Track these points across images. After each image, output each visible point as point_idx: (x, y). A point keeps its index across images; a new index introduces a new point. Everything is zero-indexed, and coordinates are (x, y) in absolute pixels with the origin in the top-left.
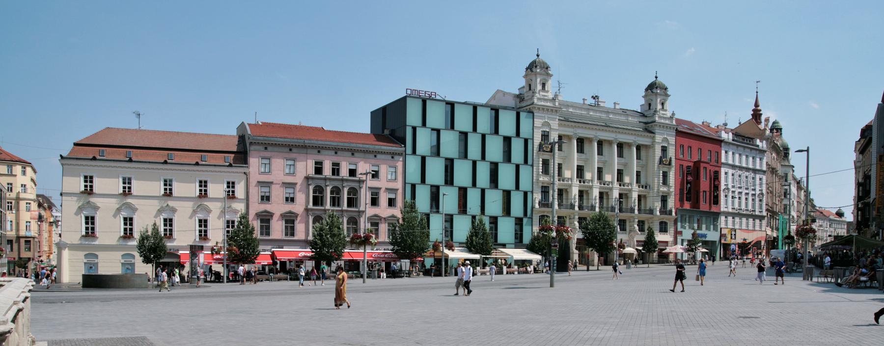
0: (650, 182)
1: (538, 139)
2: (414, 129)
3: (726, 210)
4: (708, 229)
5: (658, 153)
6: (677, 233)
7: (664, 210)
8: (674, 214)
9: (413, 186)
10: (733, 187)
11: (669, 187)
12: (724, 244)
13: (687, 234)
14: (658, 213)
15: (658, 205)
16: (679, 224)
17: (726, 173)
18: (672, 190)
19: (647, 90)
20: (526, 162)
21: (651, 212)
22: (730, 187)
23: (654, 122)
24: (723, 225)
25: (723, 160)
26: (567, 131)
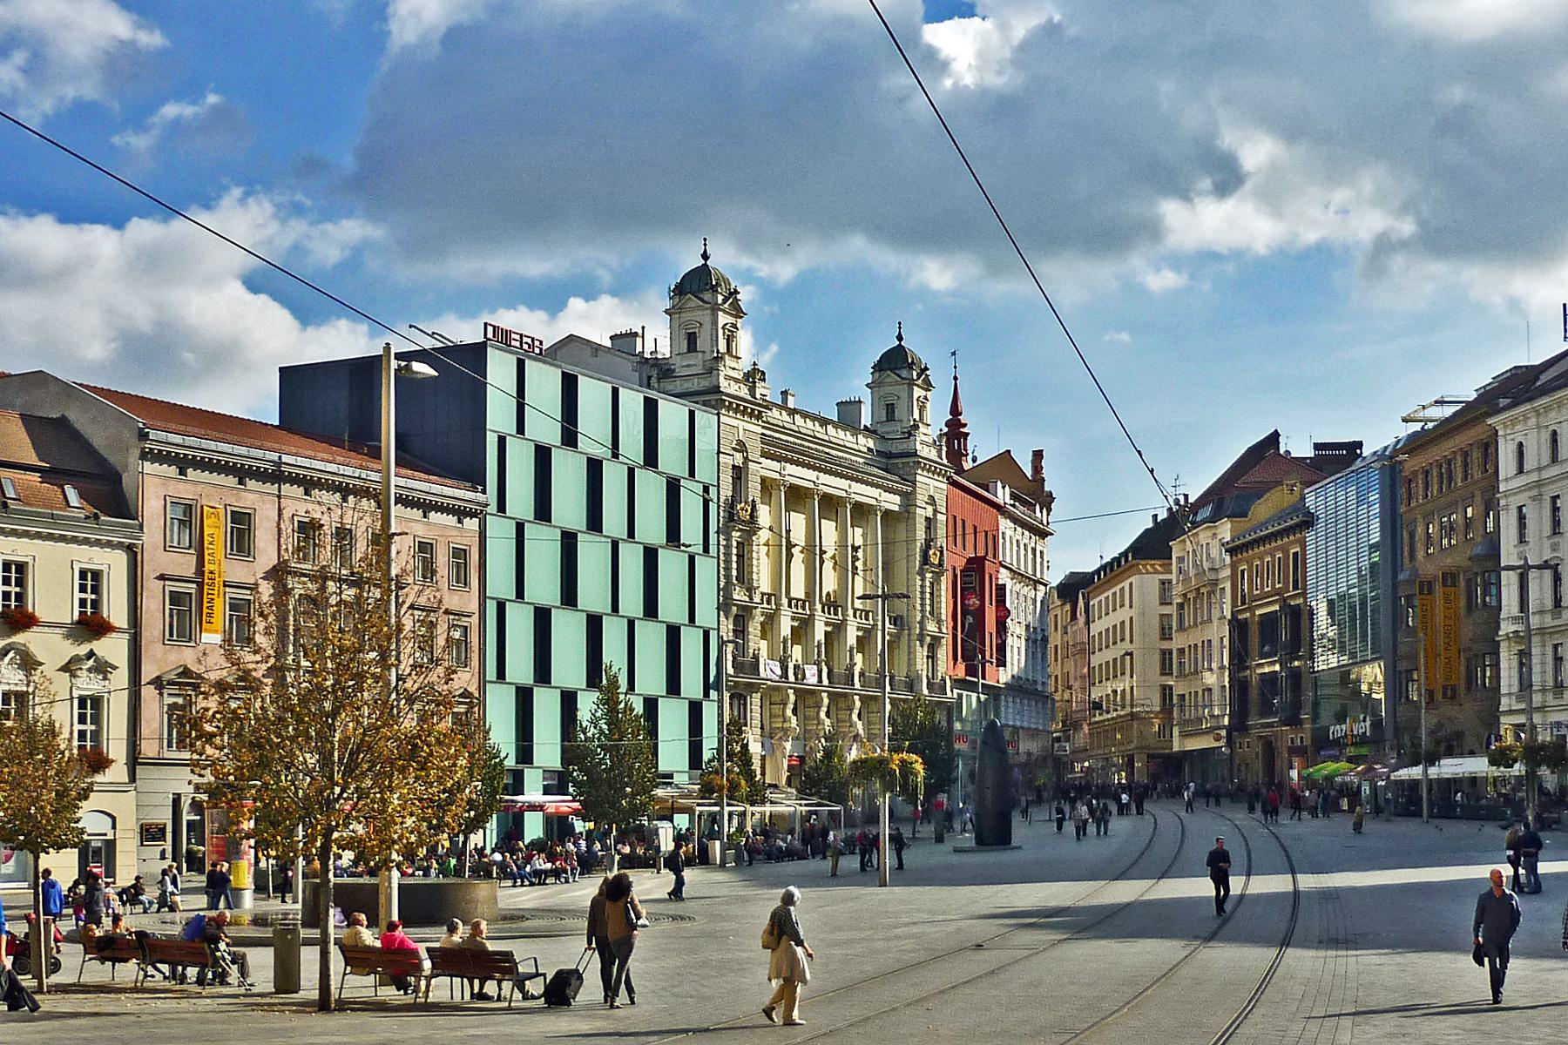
1: (726, 491)
2: (502, 441)
5: (921, 535)
9: (501, 607)
19: (879, 367)
20: (706, 550)
23: (915, 454)
26: (769, 469)
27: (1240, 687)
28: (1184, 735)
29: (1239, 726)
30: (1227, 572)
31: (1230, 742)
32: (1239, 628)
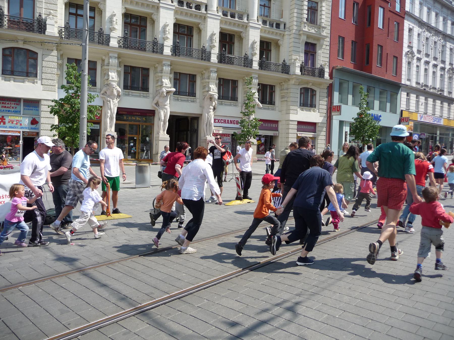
3: (408, 83)
4: (382, 108)
6: (332, 110)
7: (310, 68)
8: (327, 75)
10: (419, 52)
11: (320, 27)
13: (350, 112)
14: (298, 71)
15: (297, 60)
16: (336, 95)
17: (410, 30)
18: (326, 32)
21: (286, 69)
22: (415, 50)
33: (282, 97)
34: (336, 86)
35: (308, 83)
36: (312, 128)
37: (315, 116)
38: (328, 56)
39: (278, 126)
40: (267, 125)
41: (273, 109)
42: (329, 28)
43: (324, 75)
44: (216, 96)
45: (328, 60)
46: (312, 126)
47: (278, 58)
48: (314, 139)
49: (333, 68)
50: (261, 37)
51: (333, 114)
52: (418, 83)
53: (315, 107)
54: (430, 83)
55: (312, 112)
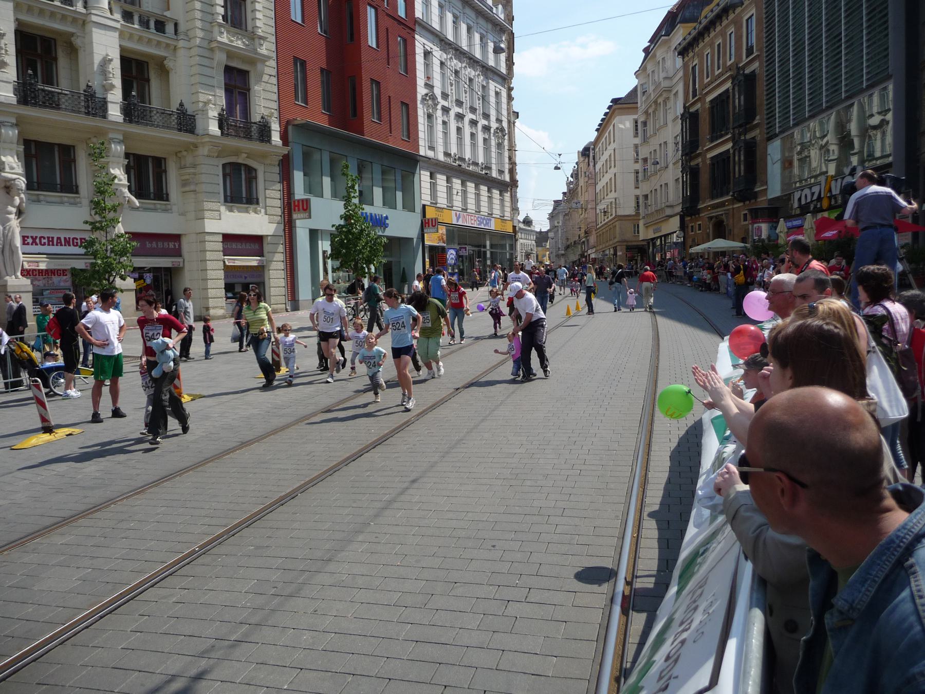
0: (177, 11)
3: (430, 154)
4: (389, 203)
6: (292, 208)
7: (238, 119)
8: (276, 138)
10: (445, 96)
11: (253, 37)
12: (432, 248)
13: (327, 212)
14: (214, 128)
16: (298, 177)
17: (427, 54)
18: (267, 48)
21: (186, 122)
22: (438, 92)
24: (426, 198)
25: (418, 14)
27: (692, 173)
28: (647, 226)
29: (690, 209)
30: (681, 74)
31: (683, 227)
32: (690, 118)
33: (185, 183)
34: (298, 159)
35: (237, 152)
36: (256, 246)
37: (258, 222)
38: (275, 97)
39: (180, 245)
40: (154, 245)
41: (166, 210)
42: (273, 39)
43: (270, 136)
44: (22, 182)
45: (275, 105)
46: (254, 243)
47: (167, 98)
48: (260, 270)
49: (288, 123)
50: (123, 49)
51: (295, 216)
52: (447, 154)
53: (258, 203)
54: (468, 155)
55: (253, 215)
